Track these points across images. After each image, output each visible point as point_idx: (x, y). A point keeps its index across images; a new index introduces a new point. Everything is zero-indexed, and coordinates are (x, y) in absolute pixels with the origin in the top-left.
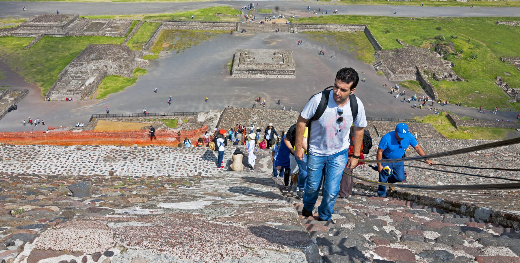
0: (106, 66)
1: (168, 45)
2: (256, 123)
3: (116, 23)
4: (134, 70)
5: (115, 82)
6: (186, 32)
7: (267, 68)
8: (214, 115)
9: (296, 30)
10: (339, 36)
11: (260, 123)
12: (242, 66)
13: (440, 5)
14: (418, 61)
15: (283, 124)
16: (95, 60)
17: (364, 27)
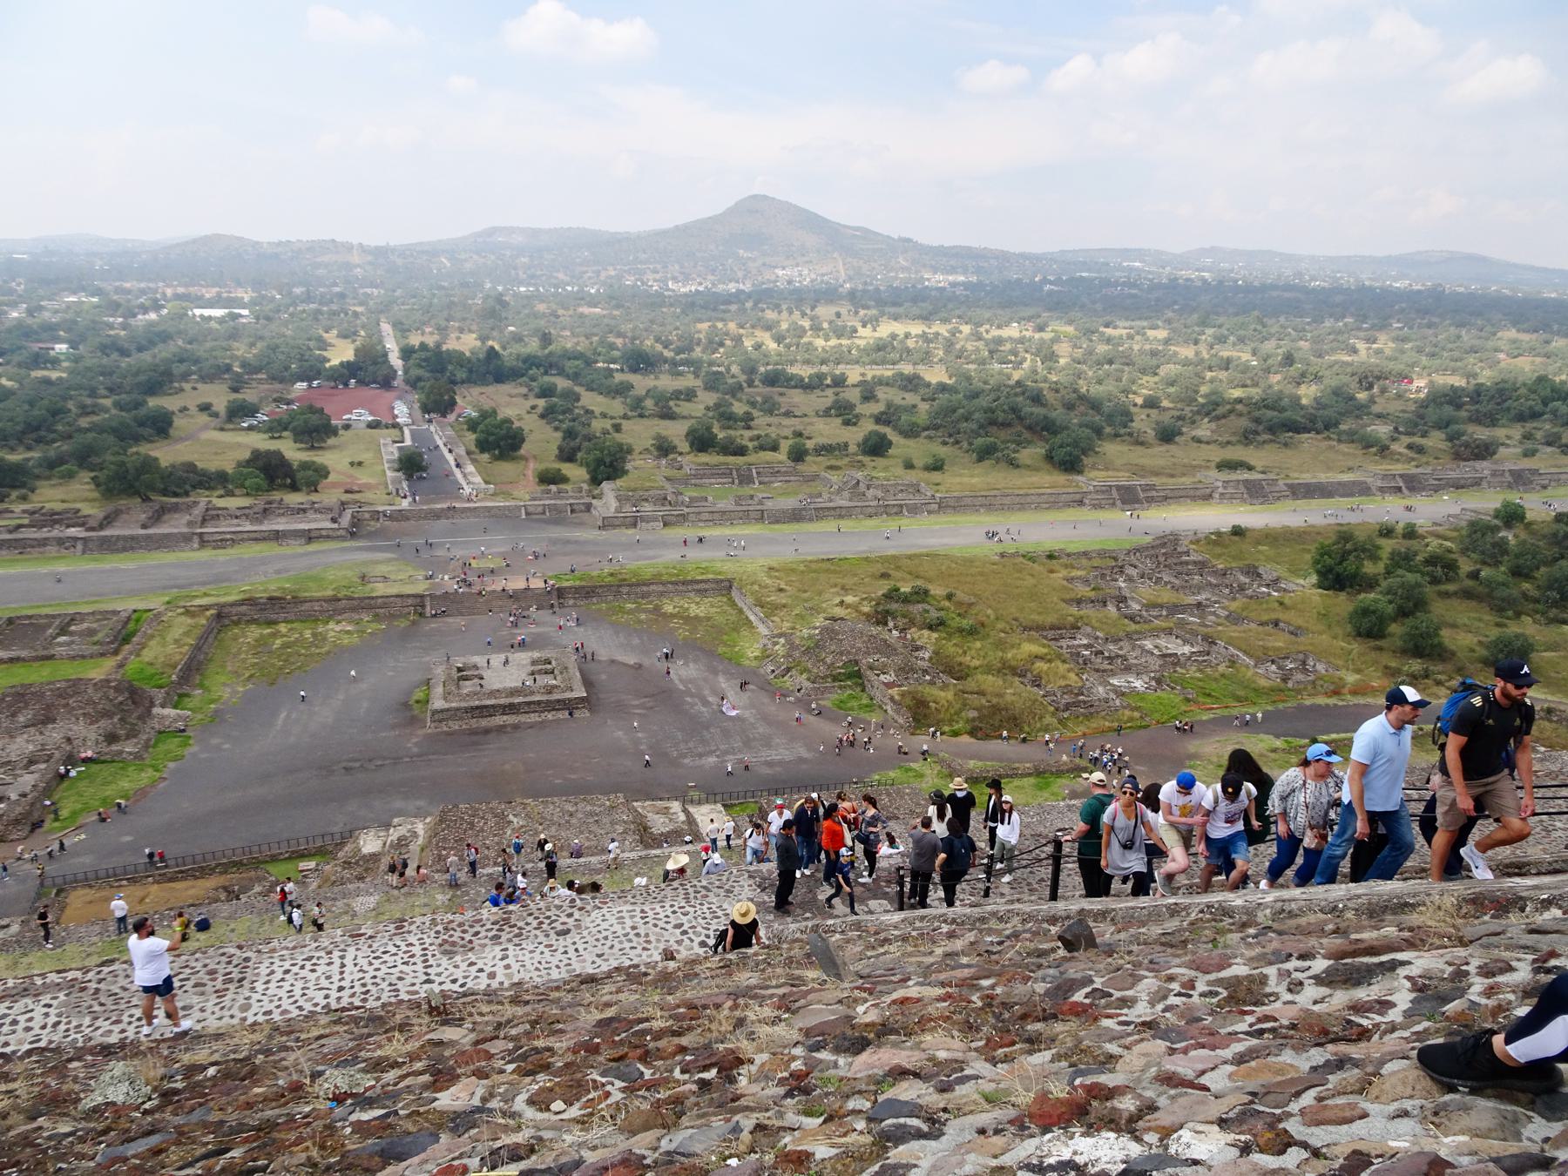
0: (69, 740)
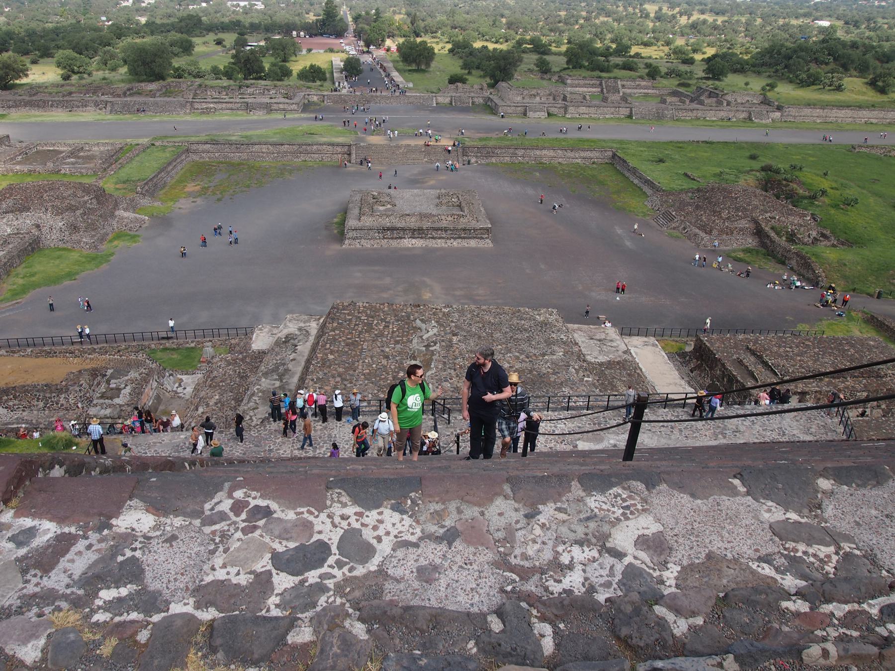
0: (38, 226)
1: (198, 187)
2: (437, 347)
3: (89, 151)
4: (110, 237)
5: (57, 262)
6: (239, 164)
7: (426, 224)
8: (300, 329)
9: (473, 160)
10: (563, 170)
11: (450, 345)
12: (367, 221)
13: (728, 126)
14: (756, 207)
15: (525, 346)
16: (12, 212)
17: (610, 154)
